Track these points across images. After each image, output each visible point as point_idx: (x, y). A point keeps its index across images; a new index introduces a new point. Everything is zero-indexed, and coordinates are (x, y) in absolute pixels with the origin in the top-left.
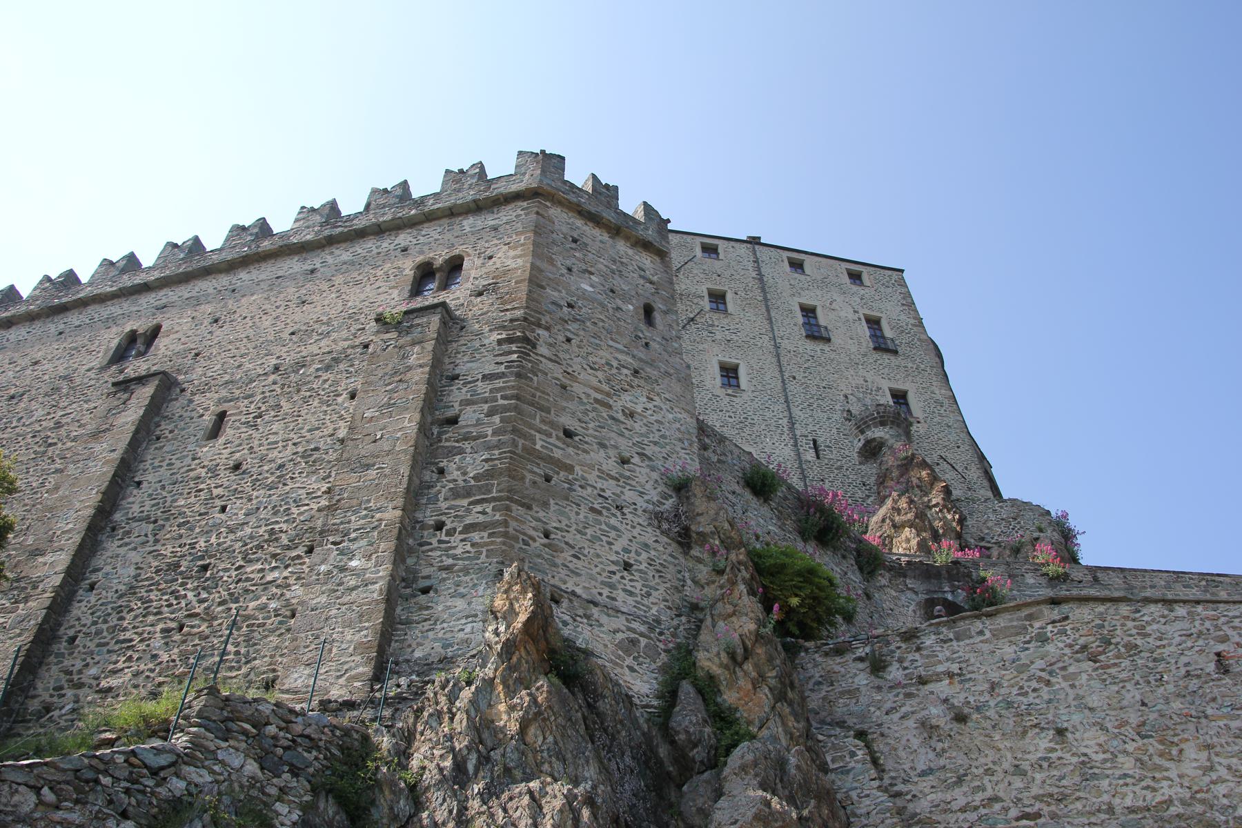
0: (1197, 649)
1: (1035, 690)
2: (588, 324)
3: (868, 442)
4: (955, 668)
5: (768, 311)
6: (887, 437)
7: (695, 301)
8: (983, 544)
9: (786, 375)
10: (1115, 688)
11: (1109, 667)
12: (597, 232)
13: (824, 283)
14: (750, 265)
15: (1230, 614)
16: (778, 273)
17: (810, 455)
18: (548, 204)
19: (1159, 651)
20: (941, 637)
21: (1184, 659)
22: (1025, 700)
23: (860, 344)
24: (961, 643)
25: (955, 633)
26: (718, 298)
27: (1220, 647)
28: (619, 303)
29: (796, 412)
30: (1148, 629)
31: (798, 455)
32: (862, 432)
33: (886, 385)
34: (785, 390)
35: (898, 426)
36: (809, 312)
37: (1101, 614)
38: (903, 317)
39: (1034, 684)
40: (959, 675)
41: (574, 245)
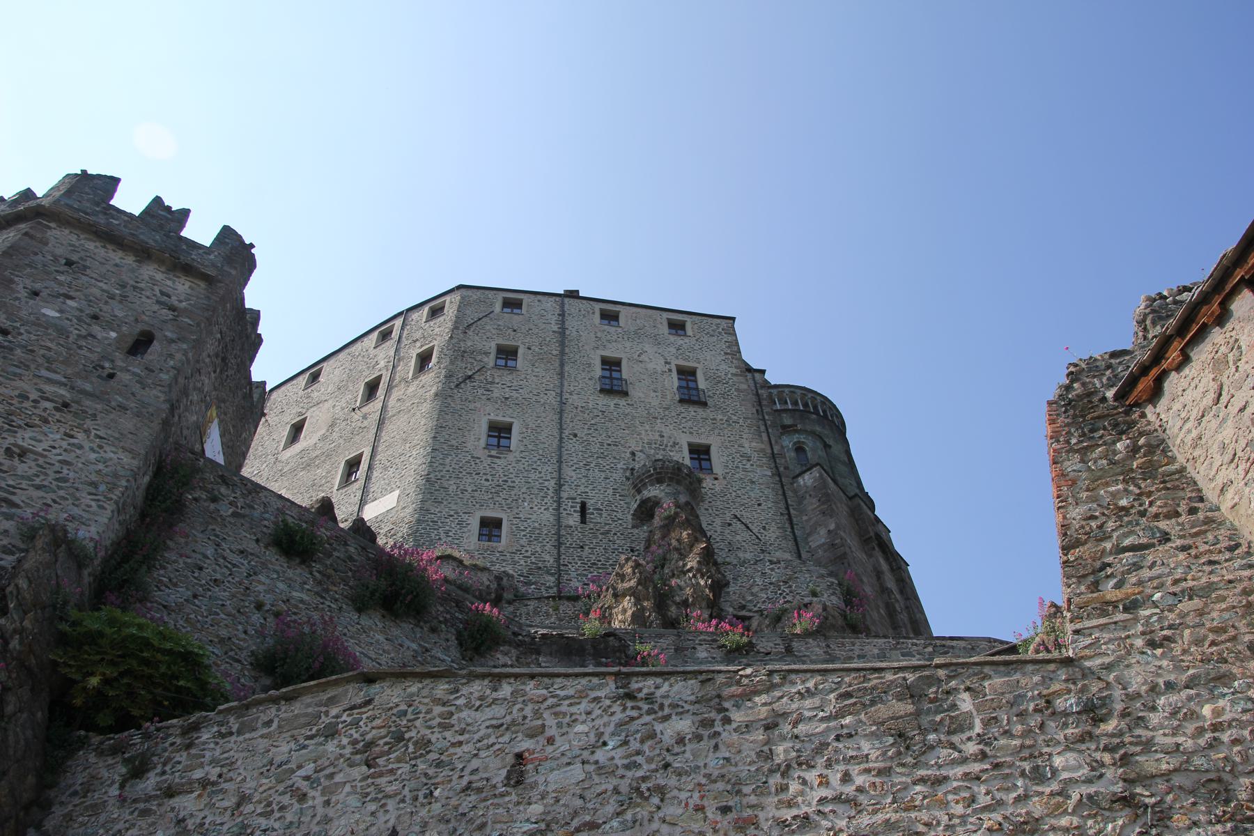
0: (497, 747)
1: (282, 808)
2: (18, 351)
3: (644, 502)
4: (214, 773)
5: (562, 365)
6: (662, 495)
7: (479, 358)
8: (744, 613)
9: (567, 432)
10: (372, 807)
11: (381, 775)
12: (116, 256)
13: (638, 334)
14: (554, 319)
15: (562, 693)
16: (585, 327)
17: (573, 520)
18: (52, 225)
19: (452, 750)
20: (223, 730)
21: (475, 763)
22: (263, 822)
23: (664, 396)
24: (241, 738)
25: (242, 724)
26: (507, 353)
27: (525, 745)
28: (96, 329)
29: (569, 473)
30: (454, 720)
31: (558, 519)
32: (639, 491)
33: (684, 440)
34: (560, 447)
35: (678, 482)
36: (611, 364)
37: (412, 695)
38: (723, 367)
39: (286, 800)
40: (214, 784)
41: (62, 268)
